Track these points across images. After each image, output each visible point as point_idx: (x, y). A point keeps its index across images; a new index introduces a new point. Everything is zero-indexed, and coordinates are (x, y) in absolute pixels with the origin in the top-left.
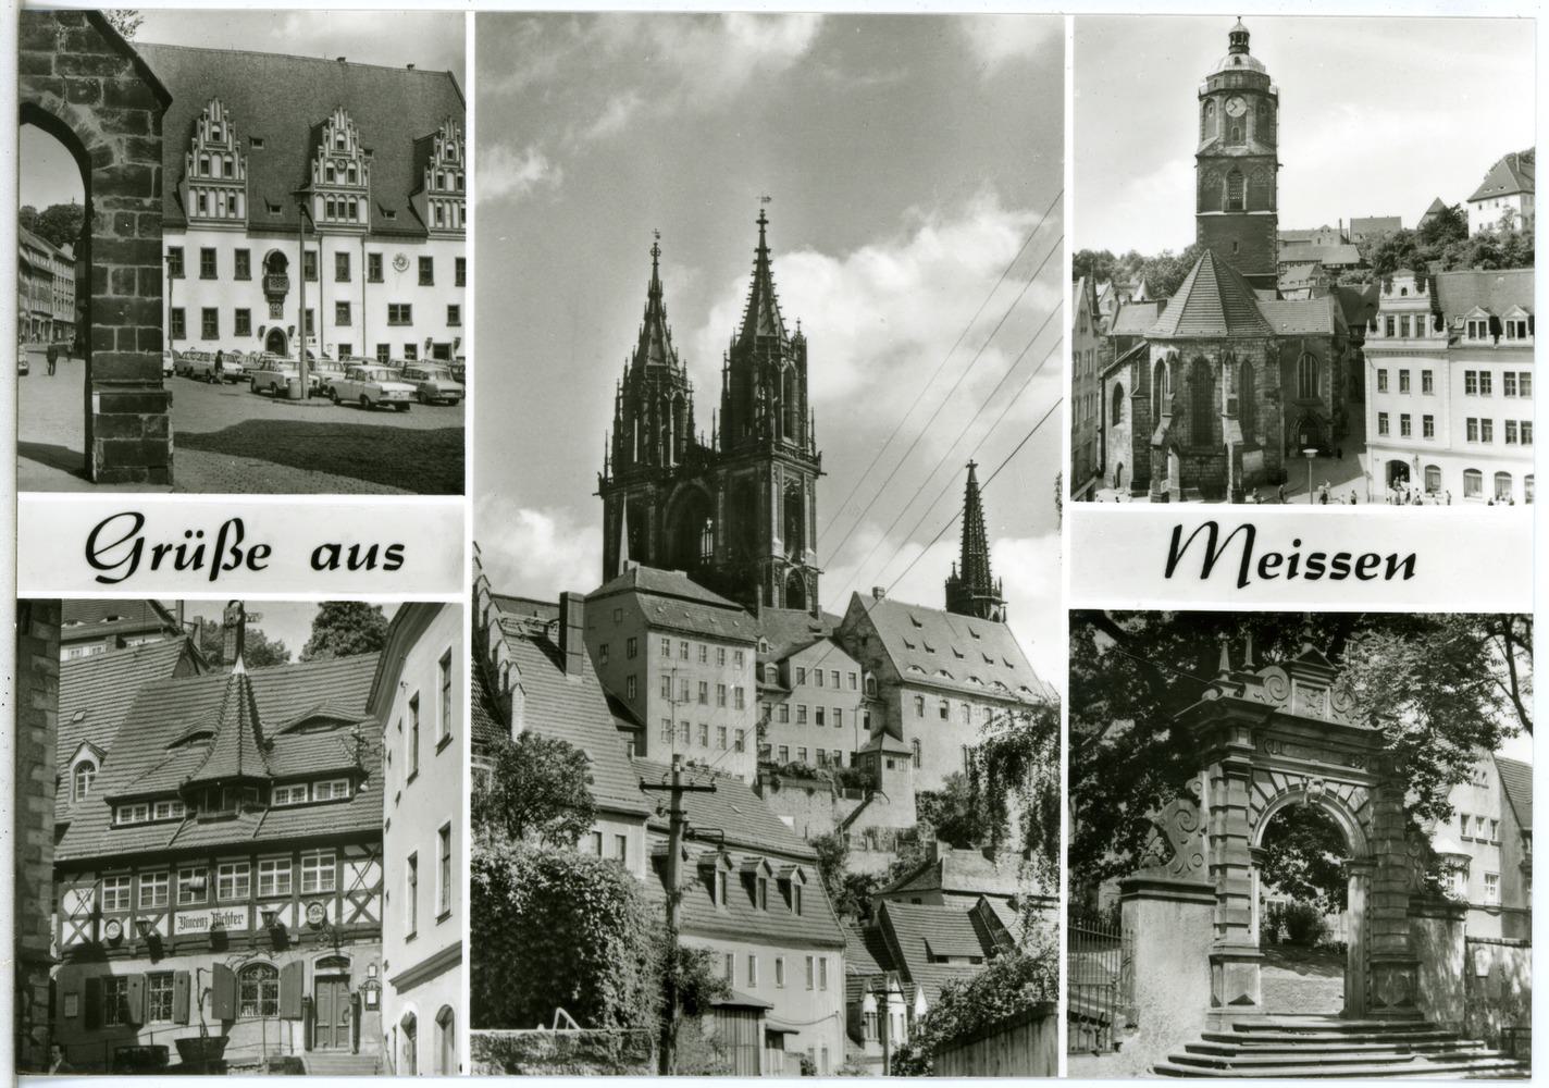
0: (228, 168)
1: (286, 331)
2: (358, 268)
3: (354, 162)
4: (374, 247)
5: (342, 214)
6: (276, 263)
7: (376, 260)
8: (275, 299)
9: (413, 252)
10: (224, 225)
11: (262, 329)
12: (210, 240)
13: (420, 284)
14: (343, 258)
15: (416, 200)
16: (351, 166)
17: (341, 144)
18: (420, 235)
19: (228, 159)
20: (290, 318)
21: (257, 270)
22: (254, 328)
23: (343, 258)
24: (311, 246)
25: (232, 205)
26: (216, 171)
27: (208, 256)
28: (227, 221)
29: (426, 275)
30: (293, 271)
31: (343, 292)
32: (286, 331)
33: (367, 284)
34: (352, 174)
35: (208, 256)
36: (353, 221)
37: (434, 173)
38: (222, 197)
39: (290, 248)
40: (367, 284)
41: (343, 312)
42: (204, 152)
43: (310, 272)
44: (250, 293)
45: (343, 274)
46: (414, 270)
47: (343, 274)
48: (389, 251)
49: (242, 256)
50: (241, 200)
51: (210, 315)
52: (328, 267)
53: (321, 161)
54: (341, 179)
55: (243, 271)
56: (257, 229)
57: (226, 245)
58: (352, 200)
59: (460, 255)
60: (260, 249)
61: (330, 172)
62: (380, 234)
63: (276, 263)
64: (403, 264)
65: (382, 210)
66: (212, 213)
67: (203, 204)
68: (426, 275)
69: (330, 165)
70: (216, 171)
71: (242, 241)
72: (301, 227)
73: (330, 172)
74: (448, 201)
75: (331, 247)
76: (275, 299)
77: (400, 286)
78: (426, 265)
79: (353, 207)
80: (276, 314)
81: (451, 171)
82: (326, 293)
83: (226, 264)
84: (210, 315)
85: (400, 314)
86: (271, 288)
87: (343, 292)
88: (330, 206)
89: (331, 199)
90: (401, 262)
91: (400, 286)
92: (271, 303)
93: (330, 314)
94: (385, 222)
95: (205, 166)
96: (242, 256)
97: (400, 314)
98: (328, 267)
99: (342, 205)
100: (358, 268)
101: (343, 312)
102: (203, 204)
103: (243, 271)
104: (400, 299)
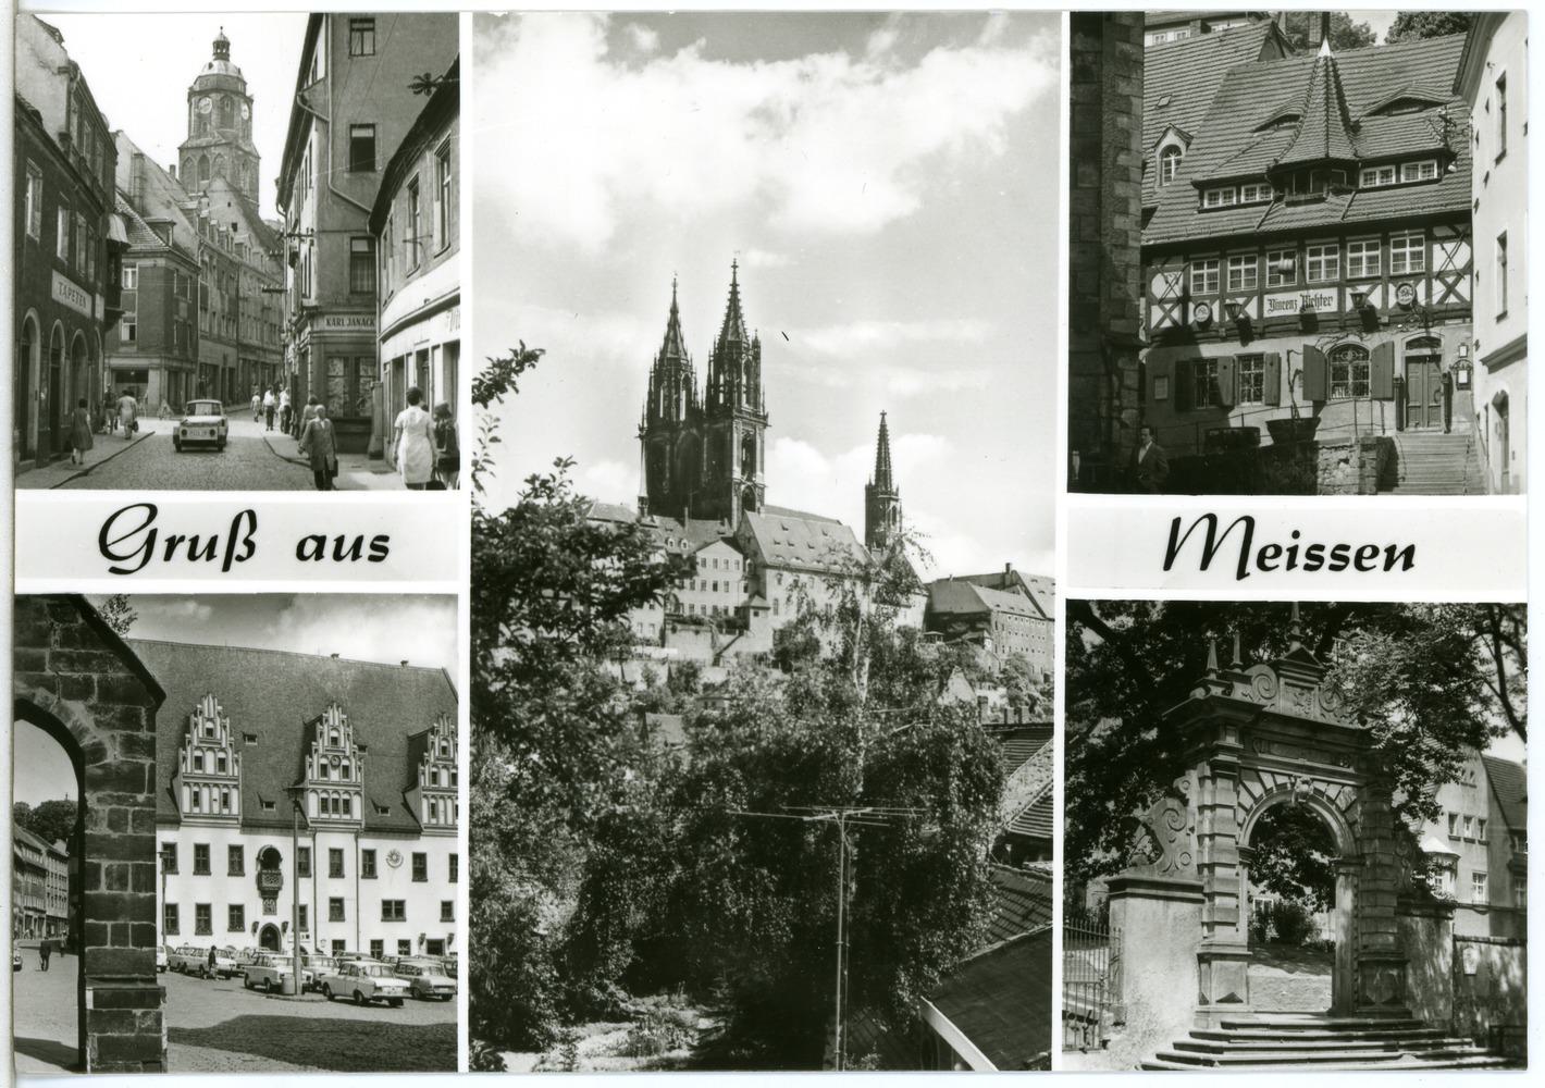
0: (222, 763)
1: (279, 926)
2: (351, 864)
3: (347, 758)
4: (367, 843)
5: (336, 810)
6: (270, 859)
7: (370, 856)
8: (269, 894)
10: (216, 821)
11: (255, 925)
12: (202, 836)
13: (414, 880)
14: (336, 854)
15: (410, 796)
16: (345, 762)
17: (335, 740)
18: (414, 831)
19: (222, 755)
20: (283, 914)
22: (248, 924)
23: (336, 854)
24: (304, 842)
25: (226, 801)
26: (210, 766)
27: (202, 852)
28: (220, 817)
29: (420, 871)
30: (287, 867)
31: (337, 888)
32: (279, 926)
33: (361, 880)
34: (346, 769)
35: (202, 852)
36: (347, 817)
38: (216, 793)
39: (283, 845)
40: (361, 880)
41: (337, 908)
42: (198, 748)
43: (303, 868)
44: (244, 891)
45: (337, 871)
46: (408, 866)
47: (337, 871)
48: (383, 847)
49: (236, 852)
50: (235, 797)
51: (203, 911)
52: (322, 863)
53: (315, 757)
54: (335, 775)
55: (236, 868)
56: (250, 825)
57: (220, 841)
58: (346, 797)
59: (453, 852)
60: (254, 845)
61: (324, 768)
62: (373, 830)
63: (270, 859)
64: (397, 860)
65: (375, 806)
66: (206, 810)
67: (196, 800)
69: (324, 761)
70: (210, 766)
71: (235, 837)
72: (293, 823)
73: (324, 768)
74: (442, 797)
75: (324, 843)
76: (269, 894)
77: (394, 882)
78: (420, 861)
79: (347, 802)
80: (269, 910)
81: (445, 767)
82: (319, 890)
83: (219, 860)
84: (203, 911)
85: (393, 910)
86: (265, 884)
87: (337, 888)
88: (324, 802)
89: (324, 795)
90: (394, 857)
91: (394, 882)
92: (265, 899)
93: (324, 909)
94: (379, 819)
95: (199, 762)
96: (236, 852)
97: (393, 910)
98: (322, 863)
99: (336, 801)
100: (351, 864)
101: (337, 908)
102: (196, 800)
104: (393, 895)
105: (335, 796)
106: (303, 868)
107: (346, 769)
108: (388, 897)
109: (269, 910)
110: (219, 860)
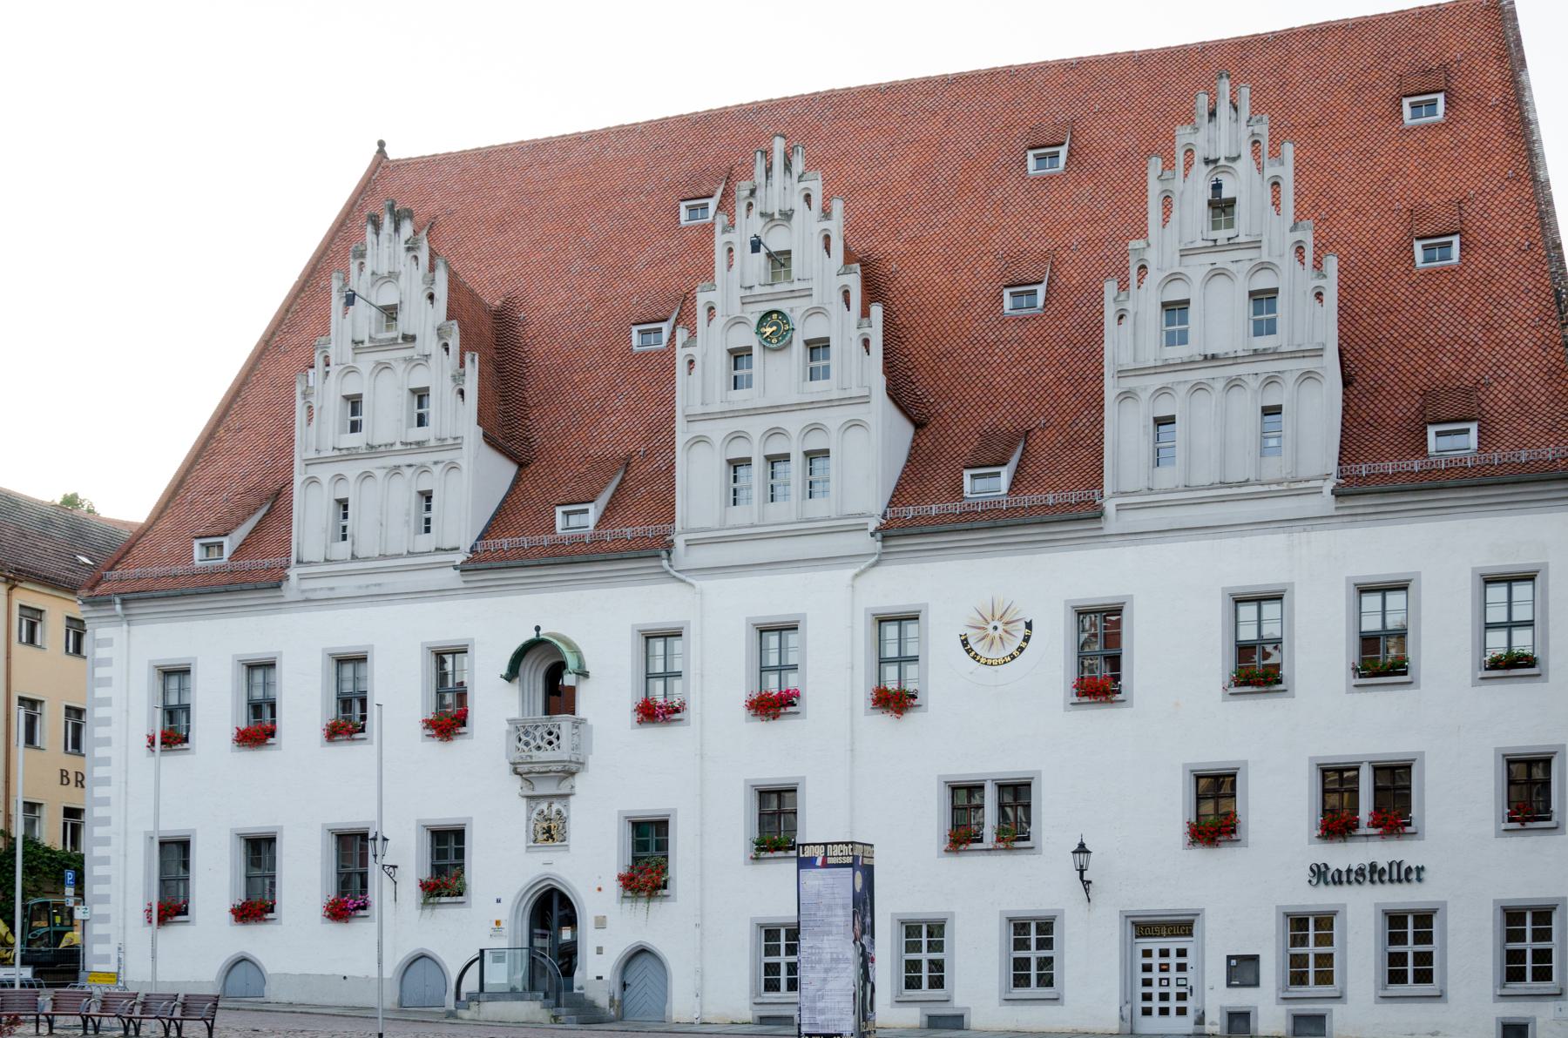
9: (1045, 581)
10: (377, 577)
12: (347, 628)
16: (815, 329)
21: (497, 704)
31: (773, 753)
34: (818, 347)
37: (1146, 302)
48: (952, 586)
61: (739, 356)
68: (1100, 676)
73: (739, 356)
80: (550, 832)
83: (401, 696)
97: (990, 814)
105: (776, 448)
107: (818, 347)
108: (967, 771)
109: (550, 832)
110: (401, 696)
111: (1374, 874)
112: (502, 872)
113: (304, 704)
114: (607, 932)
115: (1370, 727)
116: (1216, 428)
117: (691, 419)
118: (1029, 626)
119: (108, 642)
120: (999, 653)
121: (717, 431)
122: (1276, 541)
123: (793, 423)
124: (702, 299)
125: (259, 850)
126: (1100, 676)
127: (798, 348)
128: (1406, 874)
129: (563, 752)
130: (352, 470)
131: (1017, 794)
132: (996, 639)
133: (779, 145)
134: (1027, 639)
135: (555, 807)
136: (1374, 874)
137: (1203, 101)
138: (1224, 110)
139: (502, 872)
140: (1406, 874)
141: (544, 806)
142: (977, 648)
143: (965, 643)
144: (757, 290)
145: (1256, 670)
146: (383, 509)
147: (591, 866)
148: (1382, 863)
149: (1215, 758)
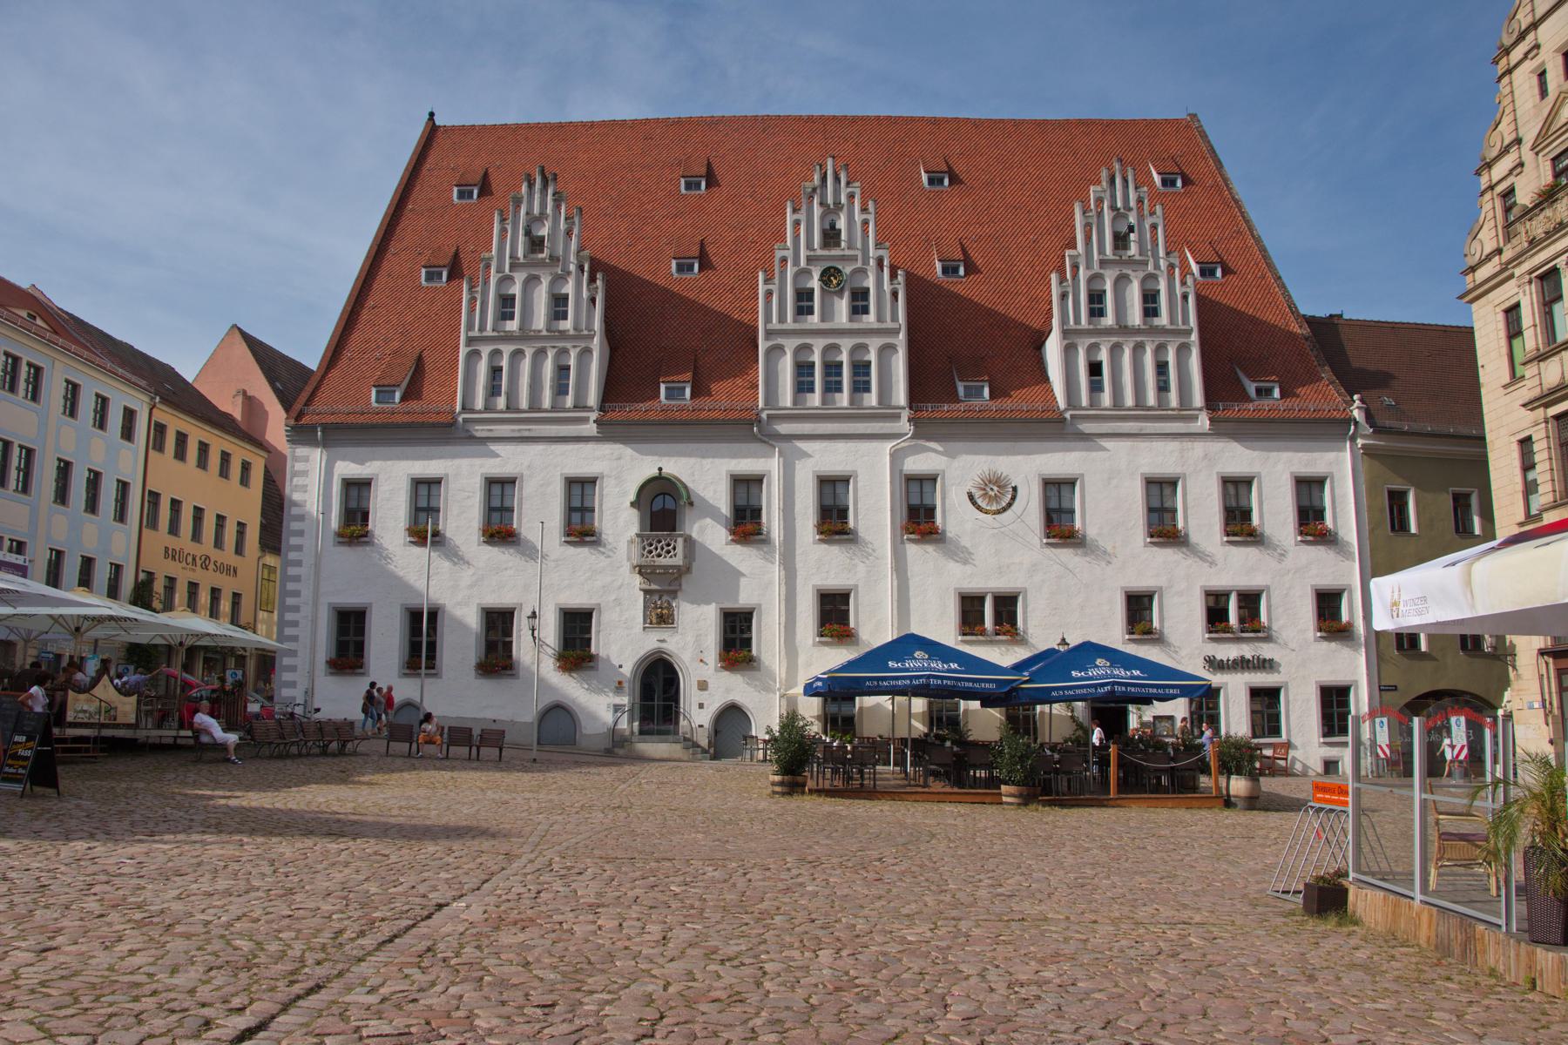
2: (875, 509)
17: (831, 236)
18: (1053, 427)
21: (619, 519)
41: (834, 612)
45: (834, 520)
49: (580, 490)
55: (581, 528)
60: (623, 470)
63: (662, 506)
68: (1059, 525)
73: (804, 296)
79: (861, 369)
80: (661, 617)
83: (541, 513)
100: (875, 509)
103: (581, 528)
104: (987, 580)
106: (746, 521)
108: (974, 585)
109: (661, 617)
110: (541, 513)
111: (1242, 664)
112: (623, 641)
113: (462, 515)
114: (706, 691)
115: (1237, 568)
116: (1130, 373)
117: (769, 334)
118: (1015, 489)
119: (307, 459)
120: (994, 507)
121: (790, 344)
122: (1173, 445)
123: (846, 344)
124: (779, 254)
125: (498, 622)
126: (1059, 525)
127: (847, 294)
128: (1265, 665)
129: (678, 560)
130: (507, 349)
131: (1007, 605)
132: (995, 496)
133: (830, 162)
134: (1013, 498)
135: (665, 598)
136: (1242, 664)
137: (1104, 174)
138: (1118, 181)
139: (623, 641)
140: (1265, 665)
141: (656, 597)
142: (979, 501)
143: (971, 497)
144: (820, 252)
145: (1164, 528)
146: (530, 377)
147: (693, 639)
148: (1248, 656)
149: (1141, 583)
